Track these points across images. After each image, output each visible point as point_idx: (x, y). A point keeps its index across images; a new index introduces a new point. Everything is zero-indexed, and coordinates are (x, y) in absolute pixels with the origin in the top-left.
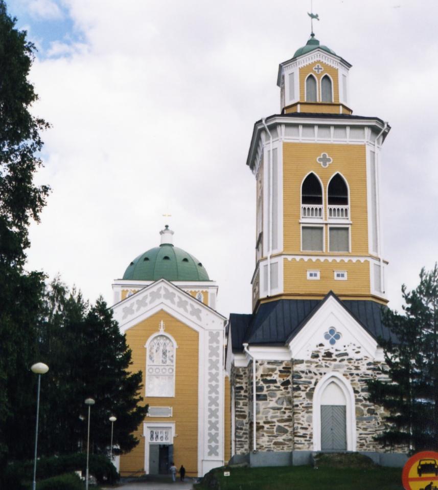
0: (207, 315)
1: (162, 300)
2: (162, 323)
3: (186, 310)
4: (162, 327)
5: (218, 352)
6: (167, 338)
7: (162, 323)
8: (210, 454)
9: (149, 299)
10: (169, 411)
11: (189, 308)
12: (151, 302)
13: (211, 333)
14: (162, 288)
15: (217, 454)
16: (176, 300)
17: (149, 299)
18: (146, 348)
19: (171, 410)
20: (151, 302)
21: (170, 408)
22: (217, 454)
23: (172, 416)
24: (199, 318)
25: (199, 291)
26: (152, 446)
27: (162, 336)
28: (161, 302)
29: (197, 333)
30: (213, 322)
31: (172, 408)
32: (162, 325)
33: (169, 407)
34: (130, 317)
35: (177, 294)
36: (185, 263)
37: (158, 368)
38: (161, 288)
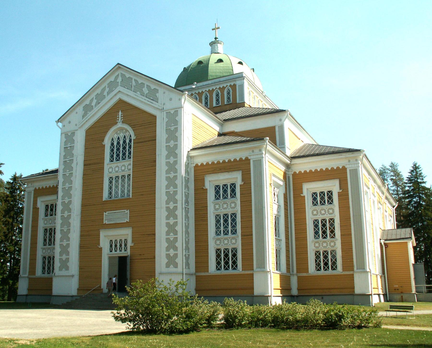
0: (164, 93)
1: (120, 88)
2: (120, 113)
6: (127, 131)
7: (120, 113)
8: (168, 266)
10: (124, 216)
12: (108, 93)
14: (120, 75)
15: (176, 266)
18: (104, 145)
19: (127, 213)
20: (108, 93)
21: (126, 212)
23: (128, 221)
25: (227, 86)
26: (110, 258)
27: (121, 129)
28: (118, 91)
30: (171, 99)
31: (128, 211)
32: (120, 116)
33: (126, 210)
34: (90, 114)
35: (134, 78)
36: (220, 64)
38: (118, 75)
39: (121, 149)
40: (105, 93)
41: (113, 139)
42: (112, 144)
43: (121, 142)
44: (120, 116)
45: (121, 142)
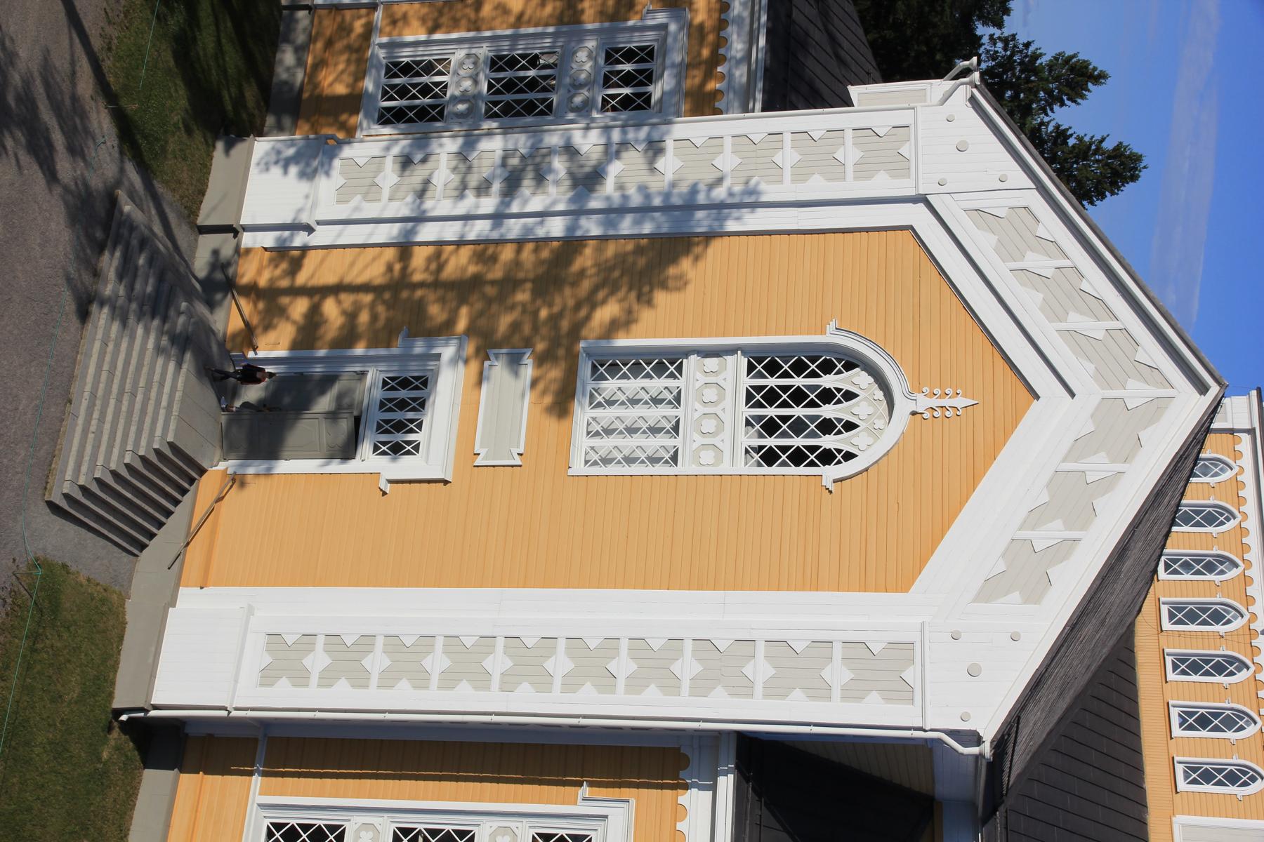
2: (961, 402)
3: (1036, 517)
4: (935, 402)
5: (797, 693)
7: (961, 402)
9: (1096, 328)
11: (1049, 534)
12: (1070, 334)
13: (903, 650)
16: (1097, 466)
17: (1096, 328)
20: (1070, 334)
22: (268, 677)
24: (990, 590)
29: (901, 580)
37: (721, 397)
39: (798, 411)
40: (1077, 321)
41: (849, 366)
42: (827, 368)
43: (827, 411)
44: (946, 402)
45: (827, 411)
